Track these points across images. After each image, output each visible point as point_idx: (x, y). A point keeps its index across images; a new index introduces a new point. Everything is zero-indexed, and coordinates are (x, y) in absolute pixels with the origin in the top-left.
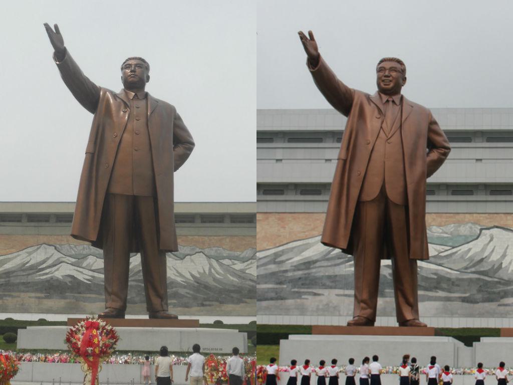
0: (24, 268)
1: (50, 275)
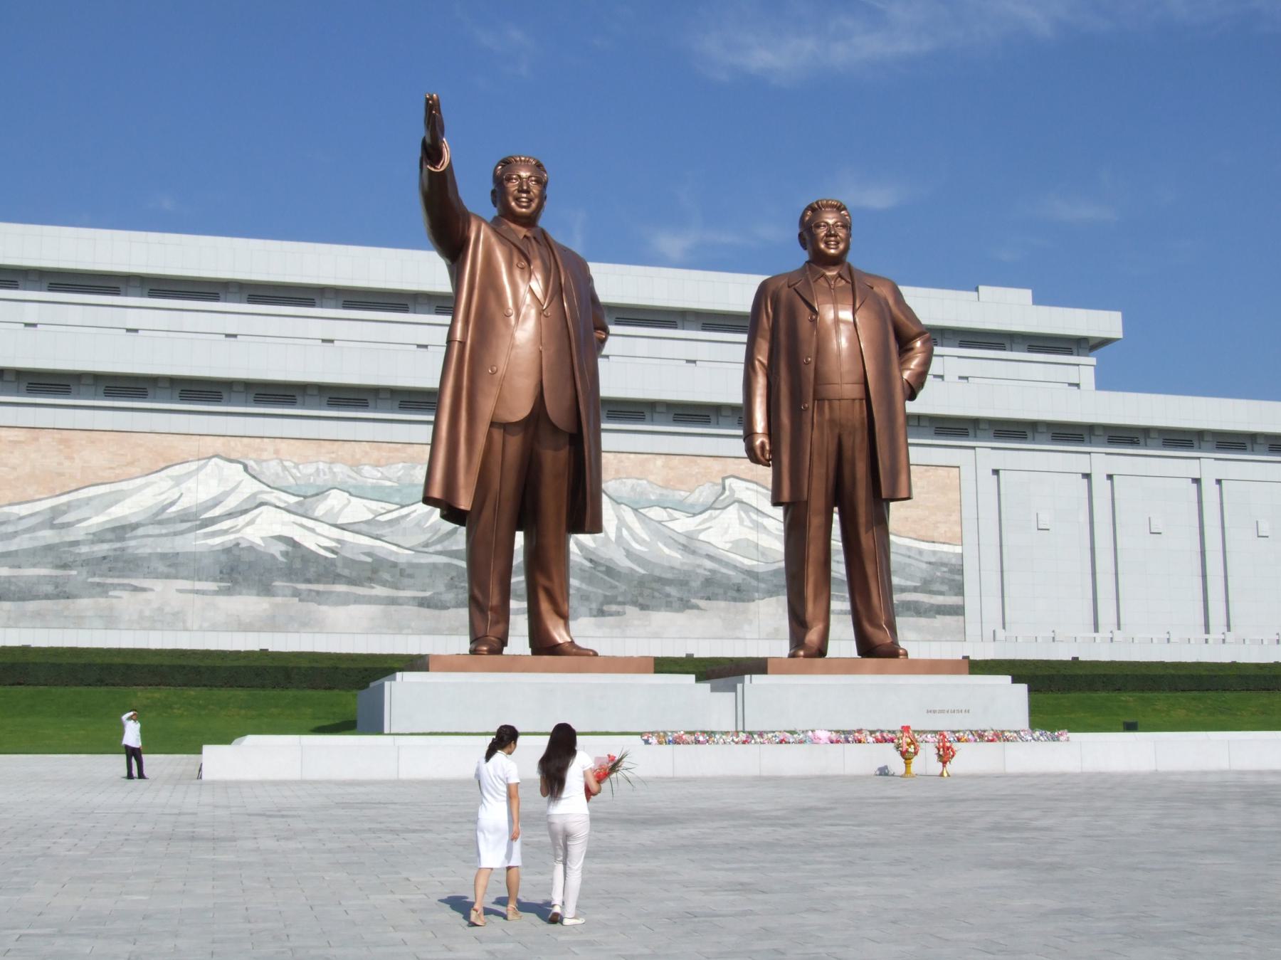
0: (164, 516)
1: (232, 537)
